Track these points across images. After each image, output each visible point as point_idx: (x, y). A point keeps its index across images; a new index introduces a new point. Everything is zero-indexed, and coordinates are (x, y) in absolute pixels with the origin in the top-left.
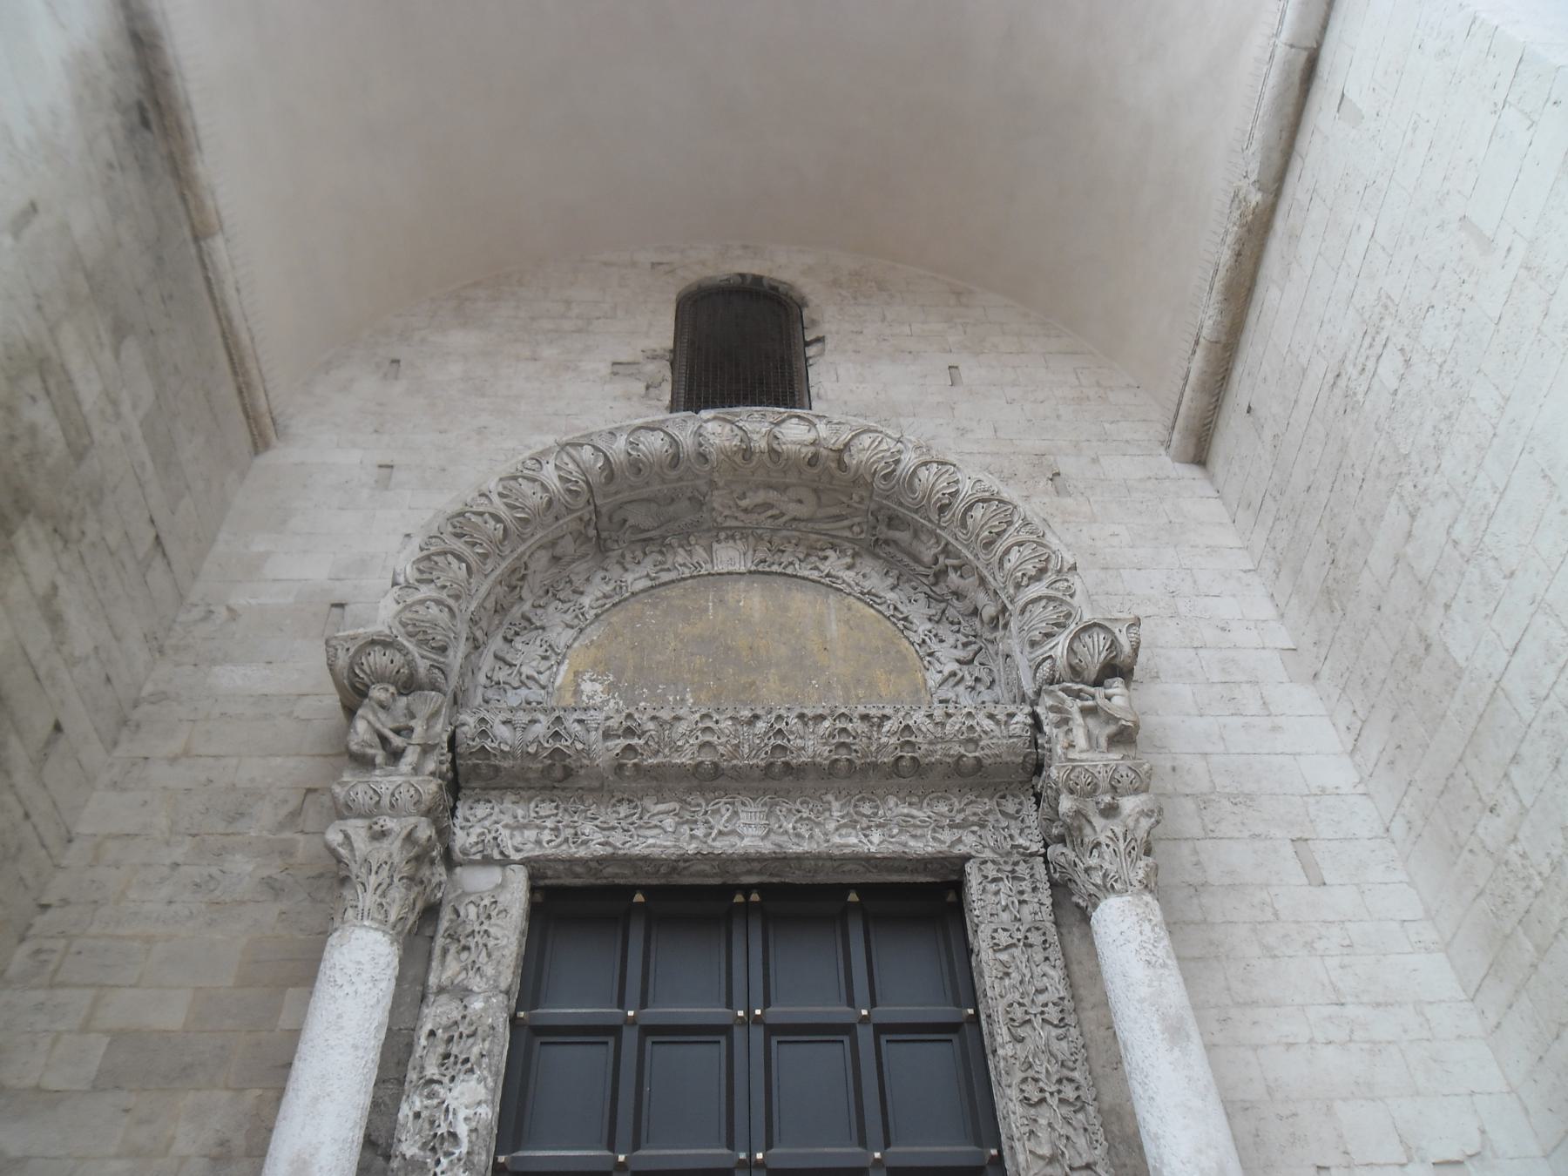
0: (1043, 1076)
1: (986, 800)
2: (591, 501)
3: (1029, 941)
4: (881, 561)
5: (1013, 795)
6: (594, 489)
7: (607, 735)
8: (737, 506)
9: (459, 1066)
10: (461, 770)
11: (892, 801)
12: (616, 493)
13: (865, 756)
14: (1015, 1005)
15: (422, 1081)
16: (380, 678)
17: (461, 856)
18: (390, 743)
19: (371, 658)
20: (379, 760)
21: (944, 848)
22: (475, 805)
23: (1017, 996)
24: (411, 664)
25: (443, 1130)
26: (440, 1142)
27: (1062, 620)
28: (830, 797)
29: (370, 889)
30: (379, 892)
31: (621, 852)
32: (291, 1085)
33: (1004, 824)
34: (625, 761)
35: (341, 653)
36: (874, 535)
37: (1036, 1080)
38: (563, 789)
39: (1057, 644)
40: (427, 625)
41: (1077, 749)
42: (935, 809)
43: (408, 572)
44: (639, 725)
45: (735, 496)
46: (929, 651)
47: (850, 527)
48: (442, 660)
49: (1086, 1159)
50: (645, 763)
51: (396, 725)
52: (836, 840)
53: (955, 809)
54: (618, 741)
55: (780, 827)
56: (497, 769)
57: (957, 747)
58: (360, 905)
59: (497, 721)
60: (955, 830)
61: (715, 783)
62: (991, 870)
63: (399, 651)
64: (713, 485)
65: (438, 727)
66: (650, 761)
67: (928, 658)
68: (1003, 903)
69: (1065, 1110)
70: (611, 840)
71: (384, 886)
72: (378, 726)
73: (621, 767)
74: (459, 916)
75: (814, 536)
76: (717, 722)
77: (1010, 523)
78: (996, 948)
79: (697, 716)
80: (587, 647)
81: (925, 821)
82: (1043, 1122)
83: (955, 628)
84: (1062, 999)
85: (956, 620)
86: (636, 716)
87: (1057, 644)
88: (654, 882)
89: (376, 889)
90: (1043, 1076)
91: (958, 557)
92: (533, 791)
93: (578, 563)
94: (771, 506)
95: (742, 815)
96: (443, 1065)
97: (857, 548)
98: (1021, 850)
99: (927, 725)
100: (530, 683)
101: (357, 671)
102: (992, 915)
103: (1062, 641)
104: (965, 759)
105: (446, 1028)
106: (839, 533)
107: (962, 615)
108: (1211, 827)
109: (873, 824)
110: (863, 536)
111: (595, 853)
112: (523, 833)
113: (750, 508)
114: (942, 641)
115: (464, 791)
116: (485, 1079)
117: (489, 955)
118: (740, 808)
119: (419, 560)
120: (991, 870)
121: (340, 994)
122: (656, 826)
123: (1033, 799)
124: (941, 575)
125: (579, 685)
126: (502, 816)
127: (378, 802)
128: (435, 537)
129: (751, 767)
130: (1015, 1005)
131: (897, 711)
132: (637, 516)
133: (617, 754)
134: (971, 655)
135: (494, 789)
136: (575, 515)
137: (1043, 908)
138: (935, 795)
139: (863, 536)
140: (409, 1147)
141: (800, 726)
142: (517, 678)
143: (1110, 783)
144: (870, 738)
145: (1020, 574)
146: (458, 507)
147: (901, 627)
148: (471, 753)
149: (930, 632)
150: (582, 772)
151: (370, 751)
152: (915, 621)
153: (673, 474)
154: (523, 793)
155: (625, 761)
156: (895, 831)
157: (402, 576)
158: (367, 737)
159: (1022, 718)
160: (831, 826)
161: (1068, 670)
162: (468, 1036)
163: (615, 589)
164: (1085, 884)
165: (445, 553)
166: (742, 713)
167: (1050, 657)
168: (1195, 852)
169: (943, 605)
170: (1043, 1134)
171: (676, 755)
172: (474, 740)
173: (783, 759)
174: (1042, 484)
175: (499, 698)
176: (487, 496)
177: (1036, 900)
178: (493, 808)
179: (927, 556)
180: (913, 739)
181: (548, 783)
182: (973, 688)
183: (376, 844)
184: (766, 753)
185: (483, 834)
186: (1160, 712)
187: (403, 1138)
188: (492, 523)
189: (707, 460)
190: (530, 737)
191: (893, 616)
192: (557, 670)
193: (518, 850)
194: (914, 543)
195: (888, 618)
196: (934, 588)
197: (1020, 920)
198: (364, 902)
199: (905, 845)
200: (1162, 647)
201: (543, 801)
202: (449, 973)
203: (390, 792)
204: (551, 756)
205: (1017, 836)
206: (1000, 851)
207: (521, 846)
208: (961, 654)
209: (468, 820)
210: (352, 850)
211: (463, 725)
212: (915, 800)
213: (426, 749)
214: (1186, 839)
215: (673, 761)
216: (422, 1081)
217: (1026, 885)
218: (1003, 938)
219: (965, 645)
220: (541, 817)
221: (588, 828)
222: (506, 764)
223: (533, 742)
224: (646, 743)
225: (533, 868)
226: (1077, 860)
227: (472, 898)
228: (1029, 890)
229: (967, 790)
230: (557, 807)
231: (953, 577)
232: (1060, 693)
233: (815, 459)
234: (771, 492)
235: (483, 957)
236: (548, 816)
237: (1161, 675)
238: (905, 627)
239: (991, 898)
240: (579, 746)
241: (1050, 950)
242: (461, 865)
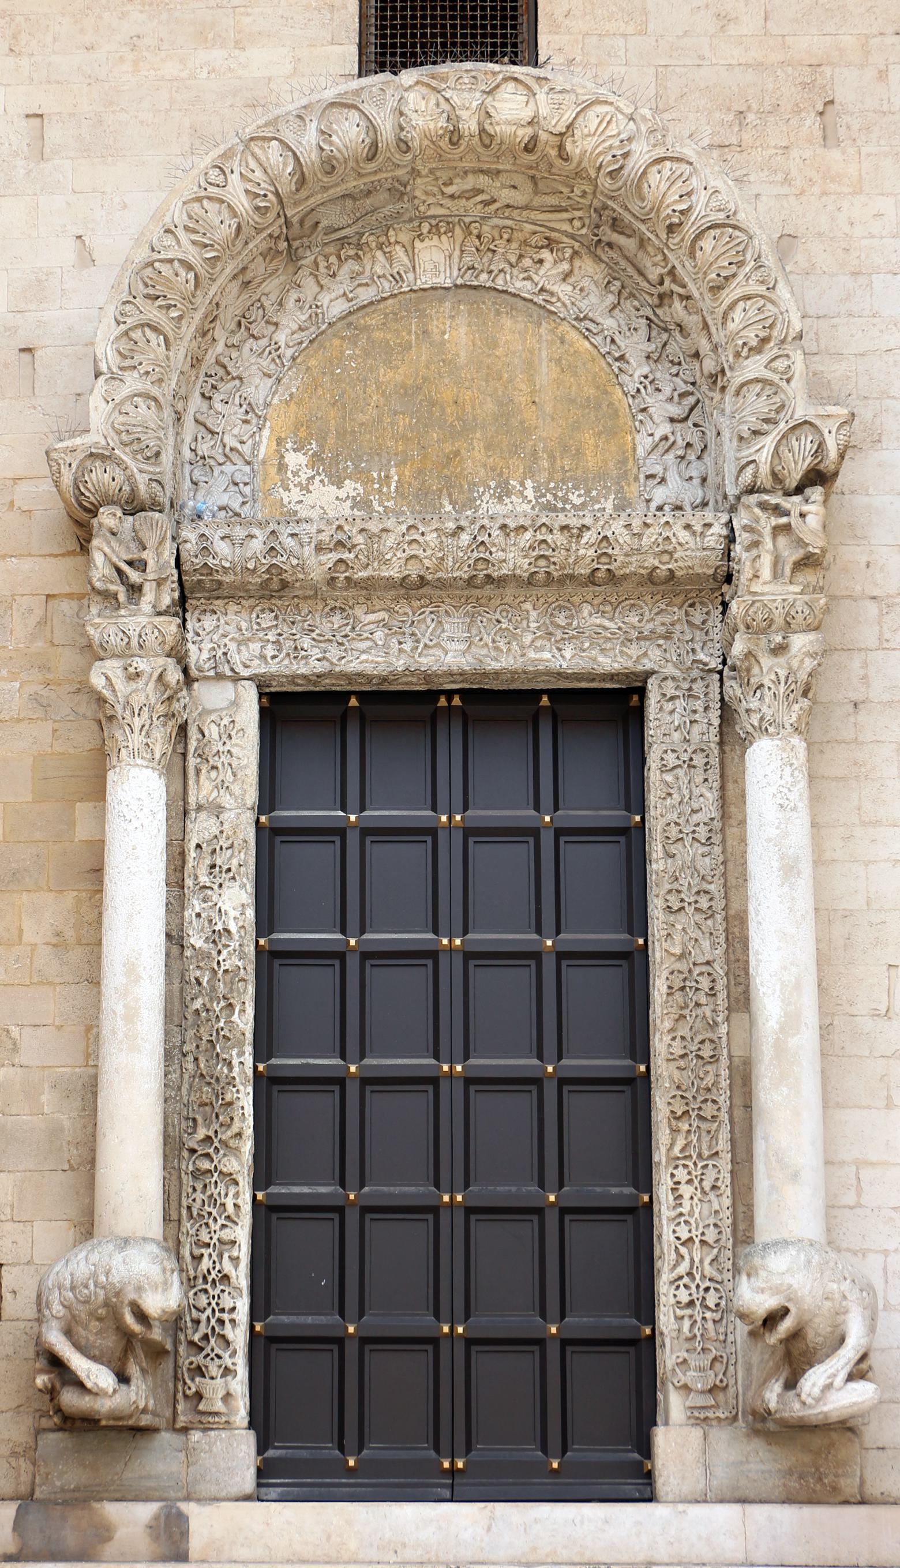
0: (685, 889)
1: (676, 609)
2: (281, 213)
3: (693, 763)
4: (603, 266)
5: (701, 603)
6: (285, 200)
7: (319, 549)
8: (443, 193)
9: (224, 875)
10: (187, 585)
11: (586, 609)
12: (308, 198)
13: (562, 568)
14: (672, 824)
15: (198, 887)
16: (109, 501)
17: (197, 672)
18: (127, 577)
20: (122, 597)
21: (630, 664)
22: (202, 617)
23: (675, 817)
24: (130, 479)
25: (219, 927)
26: (218, 937)
27: (773, 415)
28: (528, 606)
29: (137, 730)
30: (143, 733)
31: (337, 669)
32: (107, 900)
33: (688, 637)
34: (337, 575)
35: (64, 470)
36: (596, 235)
37: (679, 892)
38: (280, 598)
39: (763, 447)
40: (139, 429)
41: (761, 580)
42: (626, 620)
43: (109, 357)
44: (349, 538)
45: (440, 182)
46: (642, 407)
47: (571, 220)
48: (158, 470)
49: (708, 957)
50: (356, 576)
51: (129, 557)
52: (532, 655)
53: (646, 618)
54: (330, 555)
55: (481, 640)
56: (220, 583)
57: (651, 560)
58: (130, 745)
59: (217, 537)
60: (642, 643)
61: (420, 591)
62: (670, 689)
64: (415, 173)
65: (167, 553)
66: (360, 574)
67: (640, 417)
68: (676, 724)
69: (699, 917)
70: (327, 655)
71: (147, 727)
72: (115, 559)
73: (333, 579)
74: (204, 736)
75: (529, 227)
76: (423, 534)
77: (741, 264)
78: (664, 769)
79: (404, 527)
80: (287, 402)
81: (615, 634)
82: (679, 927)
83: (674, 370)
84: (712, 819)
85: (676, 360)
86: (346, 528)
87: (763, 447)
88: (367, 688)
89: (141, 731)
90: (685, 889)
91: (684, 286)
92: (253, 600)
93: (268, 280)
94: (482, 191)
95: (447, 627)
96: (211, 874)
97: (577, 245)
98: (701, 666)
99: (624, 537)
100: (234, 456)
101: (83, 490)
102: (664, 735)
103: (769, 442)
104: (658, 571)
105: (209, 842)
106: (557, 226)
107: (684, 353)
108: (887, 636)
109: (566, 636)
110: (584, 231)
111: (315, 670)
112: (248, 647)
113: (457, 194)
114: (658, 390)
116: (245, 885)
117: (234, 775)
118: (445, 619)
119: (117, 338)
120: (670, 689)
121: (130, 827)
122: (367, 639)
123: (720, 608)
124: (663, 298)
125: (282, 457)
127: (128, 643)
128: (128, 302)
129: (455, 579)
130: (672, 824)
131: (596, 519)
132: (330, 217)
133: (330, 569)
134: (687, 411)
136: (265, 234)
137: (712, 728)
138: (627, 602)
139: (584, 231)
140: (197, 941)
141: (501, 538)
142: (220, 451)
143: (785, 619)
144: (568, 550)
145: (740, 342)
146: (143, 254)
147: (616, 370)
148: (195, 570)
149: (646, 377)
150: (298, 585)
151: (113, 588)
152: (632, 361)
153: (372, 166)
154: (244, 602)
155: (337, 575)
156: (587, 645)
157: (104, 361)
158: (107, 572)
159: (718, 529)
160: (528, 639)
161: (770, 477)
162: (227, 849)
163: (310, 316)
164: (747, 723)
165: (142, 326)
166: (446, 525)
167: (754, 461)
168: (865, 665)
169: (665, 336)
170: (677, 938)
171: (384, 567)
172: (196, 556)
173: (485, 572)
174: (808, 122)
176: (172, 232)
177: (706, 721)
179: (654, 274)
180: (610, 551)
181: (267, 593)
182: (682, 458)
183: (134, 686)
184: (469, 566)
185: (214, 649)
186: (871, 491)
187: (191, 934)
188: (182, 272)
189: (409, 148)
190: (249, 554)
191: (609, 353)
192: (260, 436)
194: (640, 254)
195: (604, 356)
196: (658, 311)
197: (688, 741)
198: (133, 741)
199: (595, 660)
200: (894, 398)
201: (263, 611)
202: (204, 793)
203: (136, 633)
204: (268, 571)
205: (699, 650)
206: (680, 666)
207: (248, 663)
208: (675, 411)
209: (198, 635)
210: (114, 691)
211: (186, 542)
212: (608, 608)
213: (160, 582)
214: (860, 650)
215: (383, 574)
216: (198, 887)
217: (699, 705)
218: (671, 760)
219: (682, 396)
220: (263, 629)
221: (306, 642)
222: (227, 579)
224: (357, 556)
225: (260, 681)
226: (742, 697)
228: (702, 710)
229: (659, 597)
230: (276, 618)
231: (678, 305)
232: (757, 510)
233: (533, 142)
234: (481, 177)
235: (229, 777)
236: (269, 628)
237: (884, 438)
238: (620, 369)
239: (669, 719)
240: (295, 562)
241: (710, 771)
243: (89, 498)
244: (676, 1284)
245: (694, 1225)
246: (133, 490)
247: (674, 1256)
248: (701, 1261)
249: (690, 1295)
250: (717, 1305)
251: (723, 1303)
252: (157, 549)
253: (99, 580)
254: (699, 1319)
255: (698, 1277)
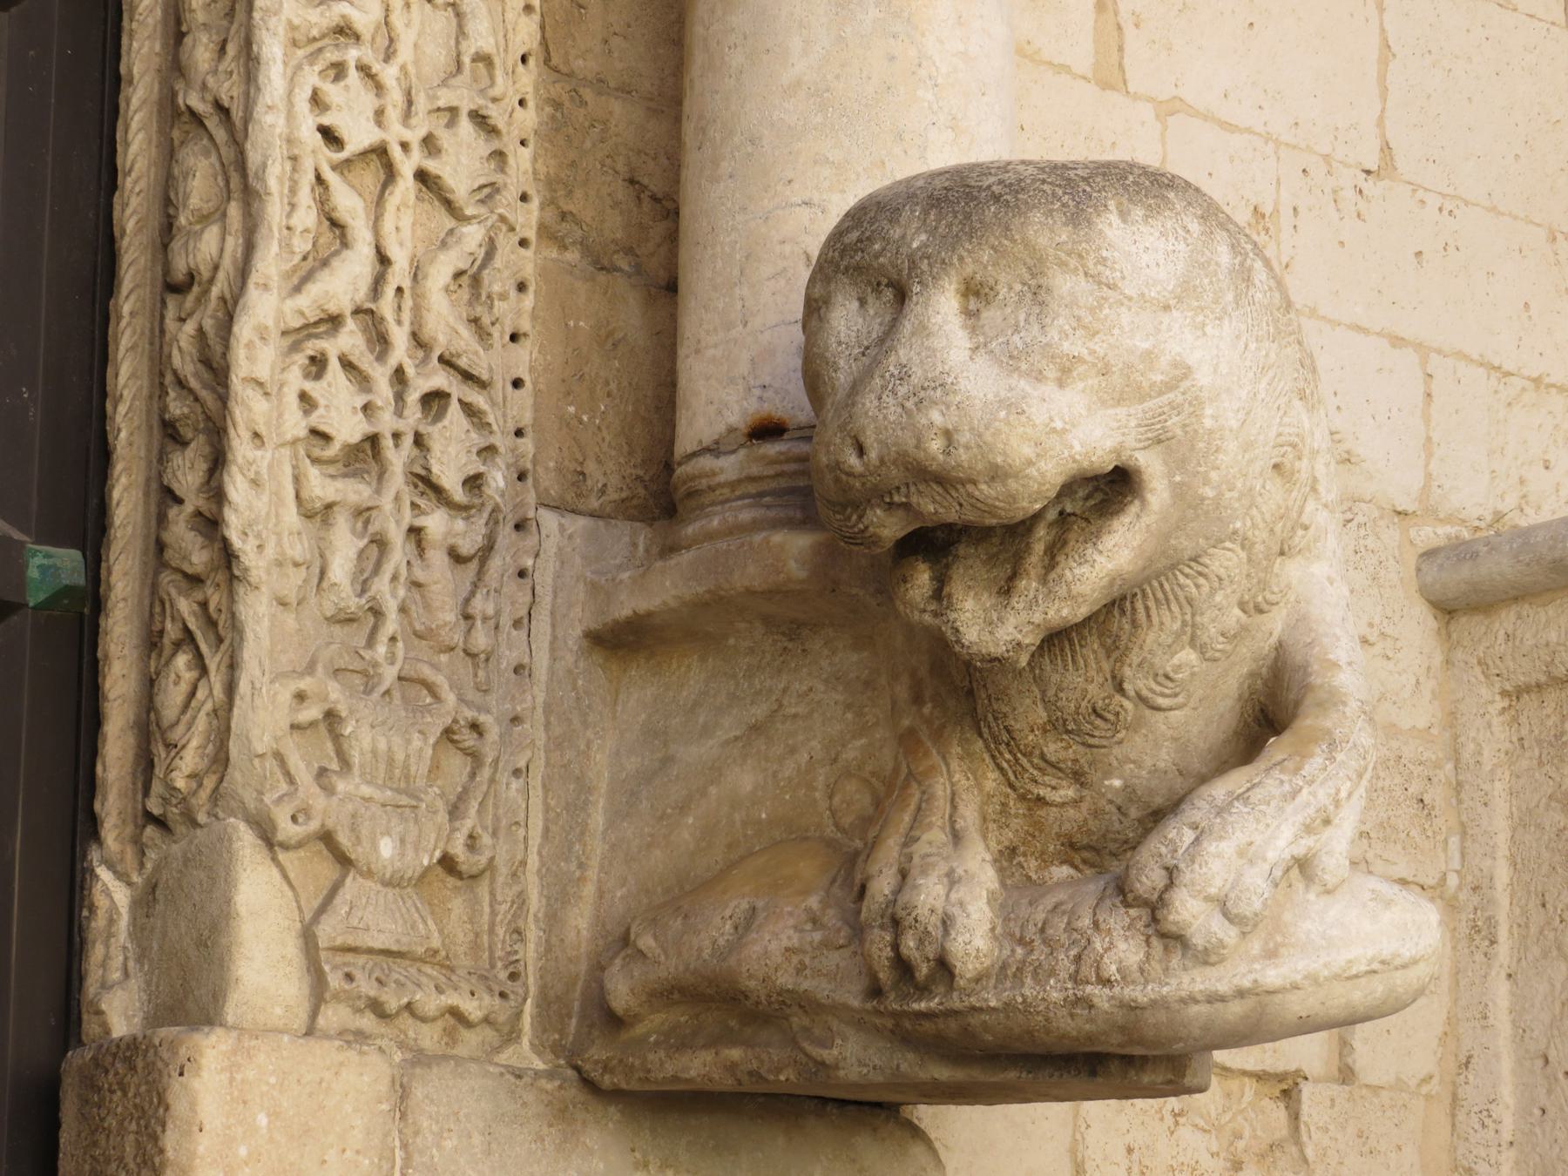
244: (311, 347)
245: (395, 96)
247: (306, 216)
248: (417, 275)
249: (367, 408)
250: (474, 482)
251: (497, 480)
254: (396, 536)
255: (400, 337)
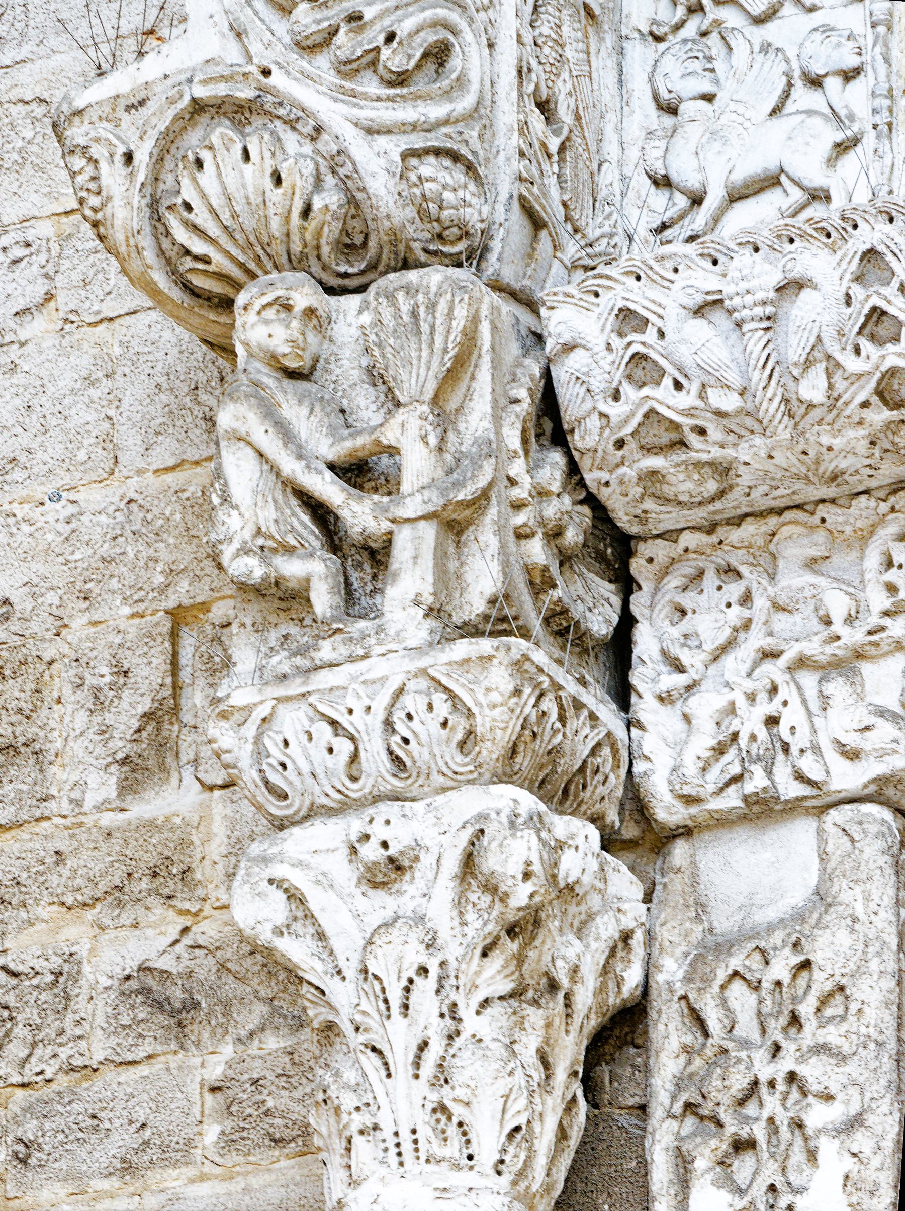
19: (207, 179)
63: (291, 124)
72: (290, 466)
115: (644, 549)
126: (781, 622)
127: (355, 758)
135: (738, 521)
158: (267, 516)
172: (616, 396)
175: (706, 87)
178: (746, 599)
193: (852, 755)
211: (568, 348)
223: (808, 363)
227: (735, 962)
242: (686, 832)
243: (206, 260)
246: (352, 201)
252: (436, 400)
253: (244, 550)
